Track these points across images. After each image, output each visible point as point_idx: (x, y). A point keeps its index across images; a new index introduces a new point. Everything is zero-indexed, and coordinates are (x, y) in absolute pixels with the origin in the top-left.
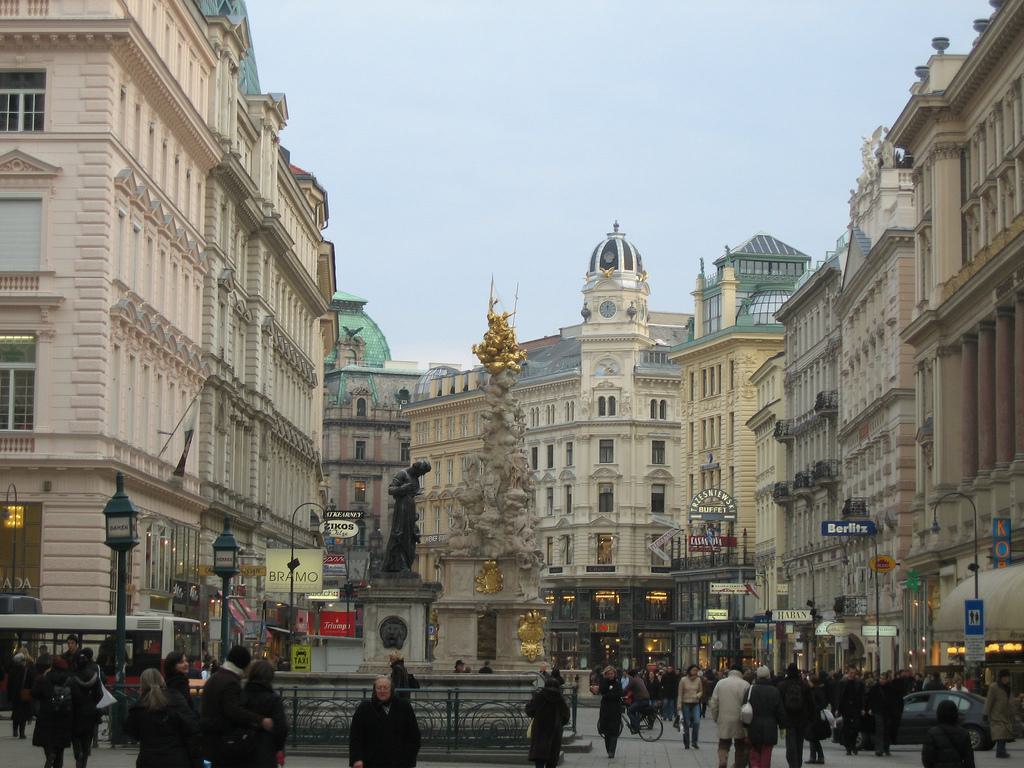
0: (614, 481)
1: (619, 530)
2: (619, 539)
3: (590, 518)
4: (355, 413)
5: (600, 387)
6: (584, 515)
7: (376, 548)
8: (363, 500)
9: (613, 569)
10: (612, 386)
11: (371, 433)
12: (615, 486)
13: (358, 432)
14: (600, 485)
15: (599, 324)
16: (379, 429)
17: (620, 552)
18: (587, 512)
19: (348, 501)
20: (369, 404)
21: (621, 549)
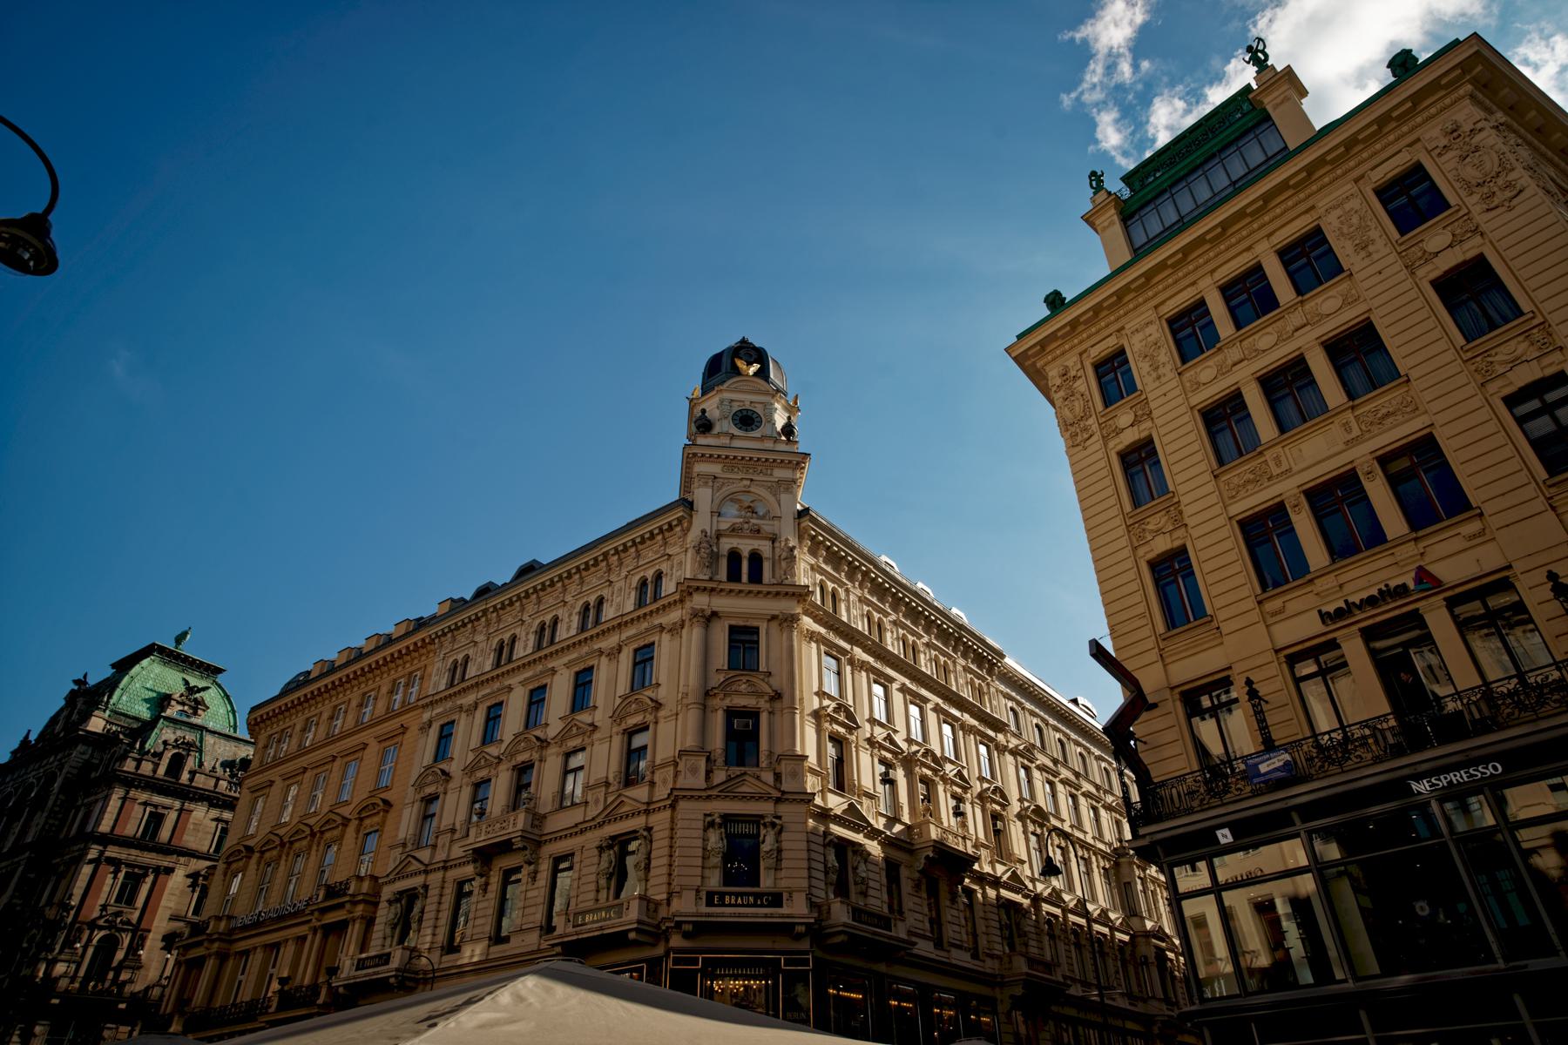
0: (763, 704)
1: (783, 809)
2: (780, 832)
3: (709, 773)
4: (162, 771)
5: (735, 531)
6: (694, 771)
7: (125, 983)
8: (131, 902)
9: (776, 900)
10: (758, 531)
11: (177, 804)
12: (764, 717)
13: (157, 799)
14: (731, 714)
15: (733, 437)
16: (192, 800)
17: (784, 864)
18: (703, 760)
19: (101, 901)
20: (191, 763)
21: (785, 855)
